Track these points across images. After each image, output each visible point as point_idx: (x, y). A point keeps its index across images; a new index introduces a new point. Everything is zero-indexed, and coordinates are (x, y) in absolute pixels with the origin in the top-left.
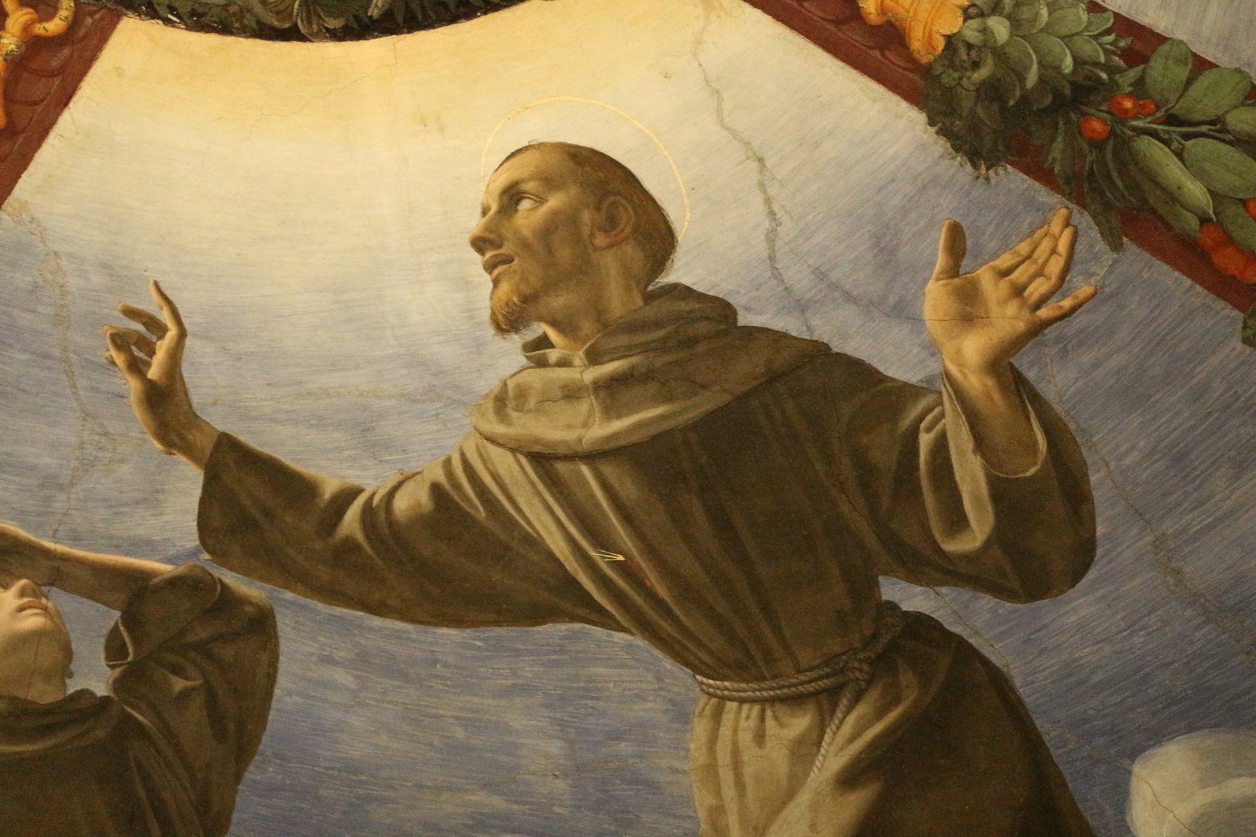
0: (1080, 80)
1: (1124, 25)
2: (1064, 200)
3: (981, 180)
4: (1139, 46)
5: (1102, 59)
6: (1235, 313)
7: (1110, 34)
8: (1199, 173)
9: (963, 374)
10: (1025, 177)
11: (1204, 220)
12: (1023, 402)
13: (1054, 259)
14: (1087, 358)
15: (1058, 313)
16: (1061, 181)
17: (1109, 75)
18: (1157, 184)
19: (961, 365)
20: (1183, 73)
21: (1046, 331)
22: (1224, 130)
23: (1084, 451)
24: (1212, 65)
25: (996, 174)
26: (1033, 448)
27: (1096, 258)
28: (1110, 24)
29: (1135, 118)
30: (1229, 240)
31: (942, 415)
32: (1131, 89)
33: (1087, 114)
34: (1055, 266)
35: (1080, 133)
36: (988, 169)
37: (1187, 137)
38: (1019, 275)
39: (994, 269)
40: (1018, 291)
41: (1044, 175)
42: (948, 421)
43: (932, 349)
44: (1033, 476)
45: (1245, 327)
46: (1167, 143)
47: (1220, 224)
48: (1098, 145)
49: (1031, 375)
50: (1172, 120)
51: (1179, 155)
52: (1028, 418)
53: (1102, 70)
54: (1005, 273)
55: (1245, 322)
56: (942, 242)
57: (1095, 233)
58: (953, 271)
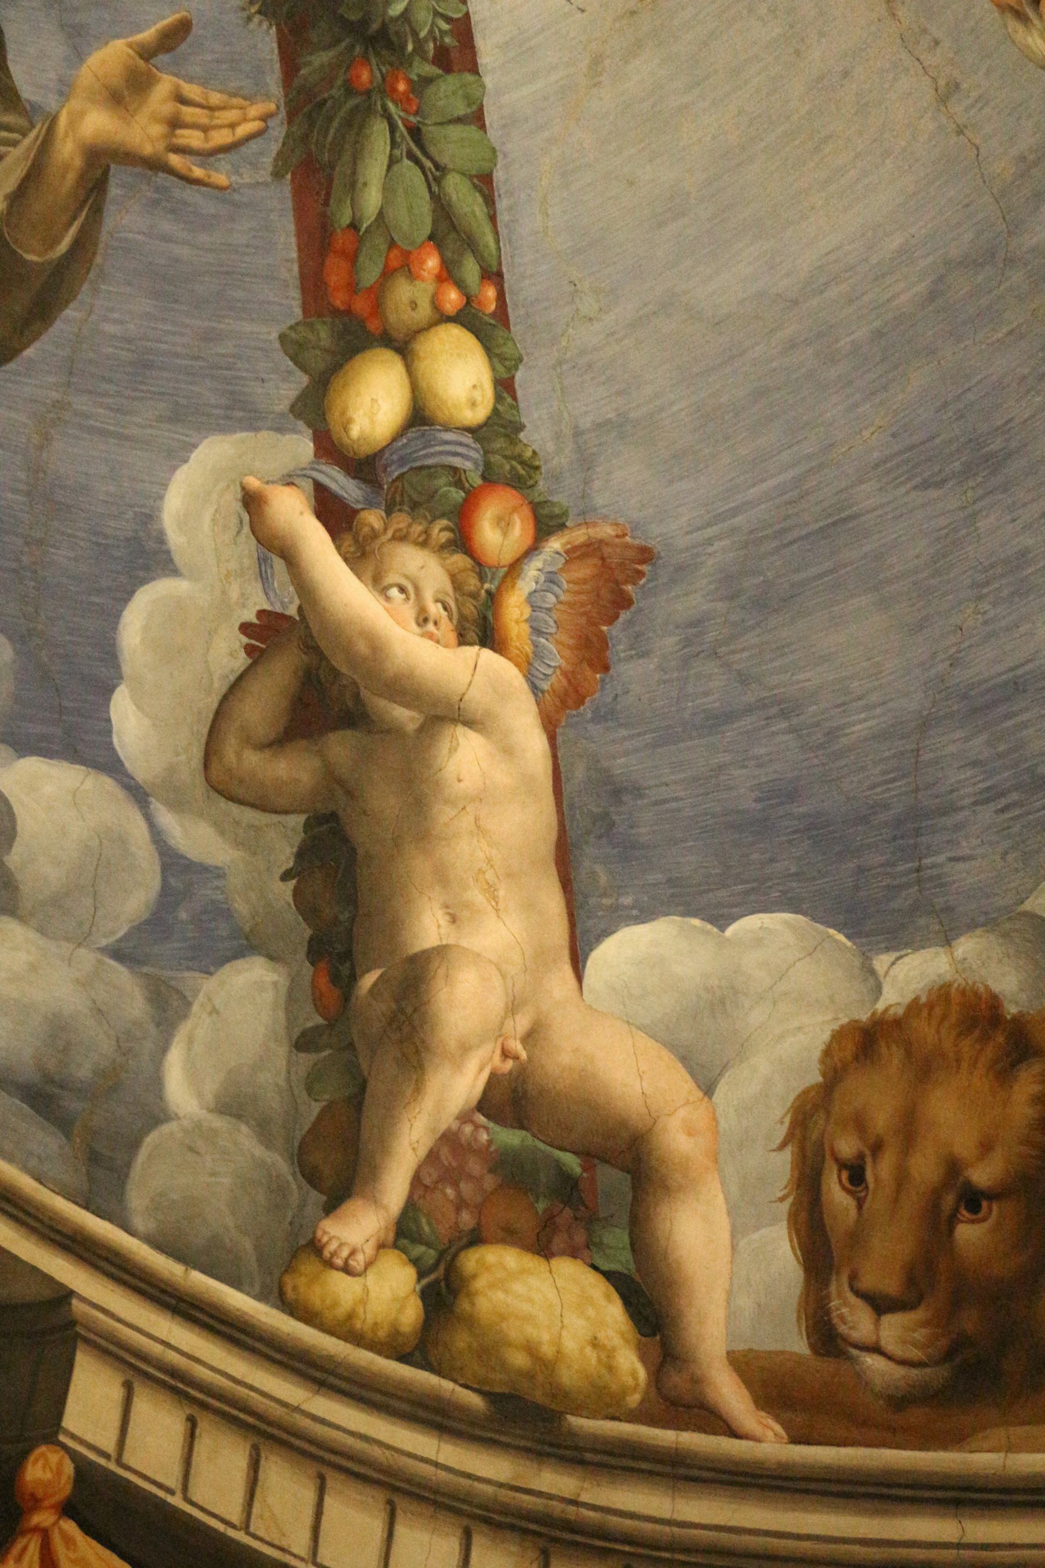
0: (392, 29)
1: (464, 29)
2: (282, 101)
3: (245, 14)
4: (454, 55)
5: (423, 34)
6: (298, 312)
7: (448, 23)
8: (388, 189)
9: (66, 133)
10: (276, 51)
11: (354, 226)
12: (85, 201)
13: (225, 132)
14: (166, 226)
15: (184, 171)
16: (296, 82)
17: (414, 50)
18: (355, 163)
19: (73, 124)
20: (461, 109)
21: (161, 174)
22: (438, 180)
23: (85, 287)
24: (483, 127)
25: (260, 23)
26: (56, 241)
27: (255, 166)
28: (456, 16)
29: (395, 102)
30: (352, 258)
31: (15, 144)
32: (416, 78)
33: (368, 60)
34: (221, 137)
35: (348, 67)
36: (259, 12)
37: (411, 156)
38: (189, 113)
39: (178, 87)
40: (175, 123)
41: (290, 67)
42: (15, 152)
43: (65, 89)
44: (26, 261)
45: (291, 328)
46: (394, 144)
47: (360, 241)
48: (350, 90)
49: (114, 191)
50: (415, 133)
51: (392, 161)
52: (74, 218)
53: (414, 42)
54: (182, 100)
55: (297, 324)
56: (165, 22)
57: (275, 147)
58: (147, 53)
